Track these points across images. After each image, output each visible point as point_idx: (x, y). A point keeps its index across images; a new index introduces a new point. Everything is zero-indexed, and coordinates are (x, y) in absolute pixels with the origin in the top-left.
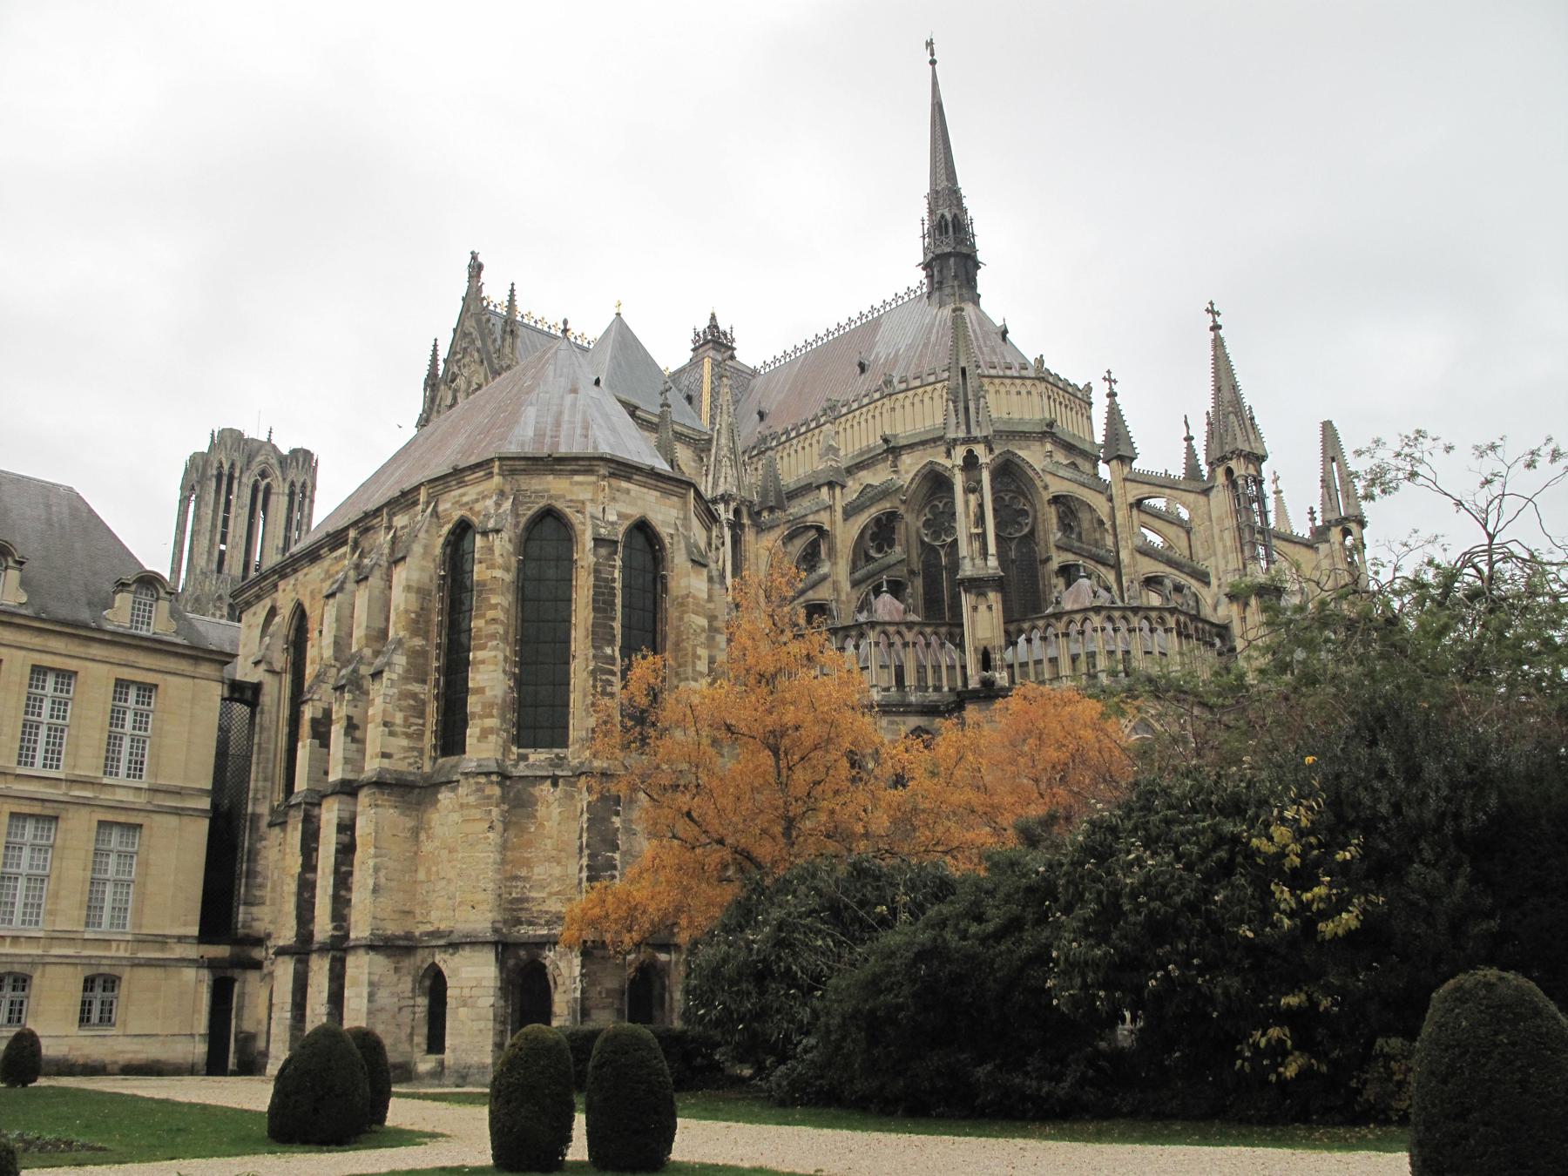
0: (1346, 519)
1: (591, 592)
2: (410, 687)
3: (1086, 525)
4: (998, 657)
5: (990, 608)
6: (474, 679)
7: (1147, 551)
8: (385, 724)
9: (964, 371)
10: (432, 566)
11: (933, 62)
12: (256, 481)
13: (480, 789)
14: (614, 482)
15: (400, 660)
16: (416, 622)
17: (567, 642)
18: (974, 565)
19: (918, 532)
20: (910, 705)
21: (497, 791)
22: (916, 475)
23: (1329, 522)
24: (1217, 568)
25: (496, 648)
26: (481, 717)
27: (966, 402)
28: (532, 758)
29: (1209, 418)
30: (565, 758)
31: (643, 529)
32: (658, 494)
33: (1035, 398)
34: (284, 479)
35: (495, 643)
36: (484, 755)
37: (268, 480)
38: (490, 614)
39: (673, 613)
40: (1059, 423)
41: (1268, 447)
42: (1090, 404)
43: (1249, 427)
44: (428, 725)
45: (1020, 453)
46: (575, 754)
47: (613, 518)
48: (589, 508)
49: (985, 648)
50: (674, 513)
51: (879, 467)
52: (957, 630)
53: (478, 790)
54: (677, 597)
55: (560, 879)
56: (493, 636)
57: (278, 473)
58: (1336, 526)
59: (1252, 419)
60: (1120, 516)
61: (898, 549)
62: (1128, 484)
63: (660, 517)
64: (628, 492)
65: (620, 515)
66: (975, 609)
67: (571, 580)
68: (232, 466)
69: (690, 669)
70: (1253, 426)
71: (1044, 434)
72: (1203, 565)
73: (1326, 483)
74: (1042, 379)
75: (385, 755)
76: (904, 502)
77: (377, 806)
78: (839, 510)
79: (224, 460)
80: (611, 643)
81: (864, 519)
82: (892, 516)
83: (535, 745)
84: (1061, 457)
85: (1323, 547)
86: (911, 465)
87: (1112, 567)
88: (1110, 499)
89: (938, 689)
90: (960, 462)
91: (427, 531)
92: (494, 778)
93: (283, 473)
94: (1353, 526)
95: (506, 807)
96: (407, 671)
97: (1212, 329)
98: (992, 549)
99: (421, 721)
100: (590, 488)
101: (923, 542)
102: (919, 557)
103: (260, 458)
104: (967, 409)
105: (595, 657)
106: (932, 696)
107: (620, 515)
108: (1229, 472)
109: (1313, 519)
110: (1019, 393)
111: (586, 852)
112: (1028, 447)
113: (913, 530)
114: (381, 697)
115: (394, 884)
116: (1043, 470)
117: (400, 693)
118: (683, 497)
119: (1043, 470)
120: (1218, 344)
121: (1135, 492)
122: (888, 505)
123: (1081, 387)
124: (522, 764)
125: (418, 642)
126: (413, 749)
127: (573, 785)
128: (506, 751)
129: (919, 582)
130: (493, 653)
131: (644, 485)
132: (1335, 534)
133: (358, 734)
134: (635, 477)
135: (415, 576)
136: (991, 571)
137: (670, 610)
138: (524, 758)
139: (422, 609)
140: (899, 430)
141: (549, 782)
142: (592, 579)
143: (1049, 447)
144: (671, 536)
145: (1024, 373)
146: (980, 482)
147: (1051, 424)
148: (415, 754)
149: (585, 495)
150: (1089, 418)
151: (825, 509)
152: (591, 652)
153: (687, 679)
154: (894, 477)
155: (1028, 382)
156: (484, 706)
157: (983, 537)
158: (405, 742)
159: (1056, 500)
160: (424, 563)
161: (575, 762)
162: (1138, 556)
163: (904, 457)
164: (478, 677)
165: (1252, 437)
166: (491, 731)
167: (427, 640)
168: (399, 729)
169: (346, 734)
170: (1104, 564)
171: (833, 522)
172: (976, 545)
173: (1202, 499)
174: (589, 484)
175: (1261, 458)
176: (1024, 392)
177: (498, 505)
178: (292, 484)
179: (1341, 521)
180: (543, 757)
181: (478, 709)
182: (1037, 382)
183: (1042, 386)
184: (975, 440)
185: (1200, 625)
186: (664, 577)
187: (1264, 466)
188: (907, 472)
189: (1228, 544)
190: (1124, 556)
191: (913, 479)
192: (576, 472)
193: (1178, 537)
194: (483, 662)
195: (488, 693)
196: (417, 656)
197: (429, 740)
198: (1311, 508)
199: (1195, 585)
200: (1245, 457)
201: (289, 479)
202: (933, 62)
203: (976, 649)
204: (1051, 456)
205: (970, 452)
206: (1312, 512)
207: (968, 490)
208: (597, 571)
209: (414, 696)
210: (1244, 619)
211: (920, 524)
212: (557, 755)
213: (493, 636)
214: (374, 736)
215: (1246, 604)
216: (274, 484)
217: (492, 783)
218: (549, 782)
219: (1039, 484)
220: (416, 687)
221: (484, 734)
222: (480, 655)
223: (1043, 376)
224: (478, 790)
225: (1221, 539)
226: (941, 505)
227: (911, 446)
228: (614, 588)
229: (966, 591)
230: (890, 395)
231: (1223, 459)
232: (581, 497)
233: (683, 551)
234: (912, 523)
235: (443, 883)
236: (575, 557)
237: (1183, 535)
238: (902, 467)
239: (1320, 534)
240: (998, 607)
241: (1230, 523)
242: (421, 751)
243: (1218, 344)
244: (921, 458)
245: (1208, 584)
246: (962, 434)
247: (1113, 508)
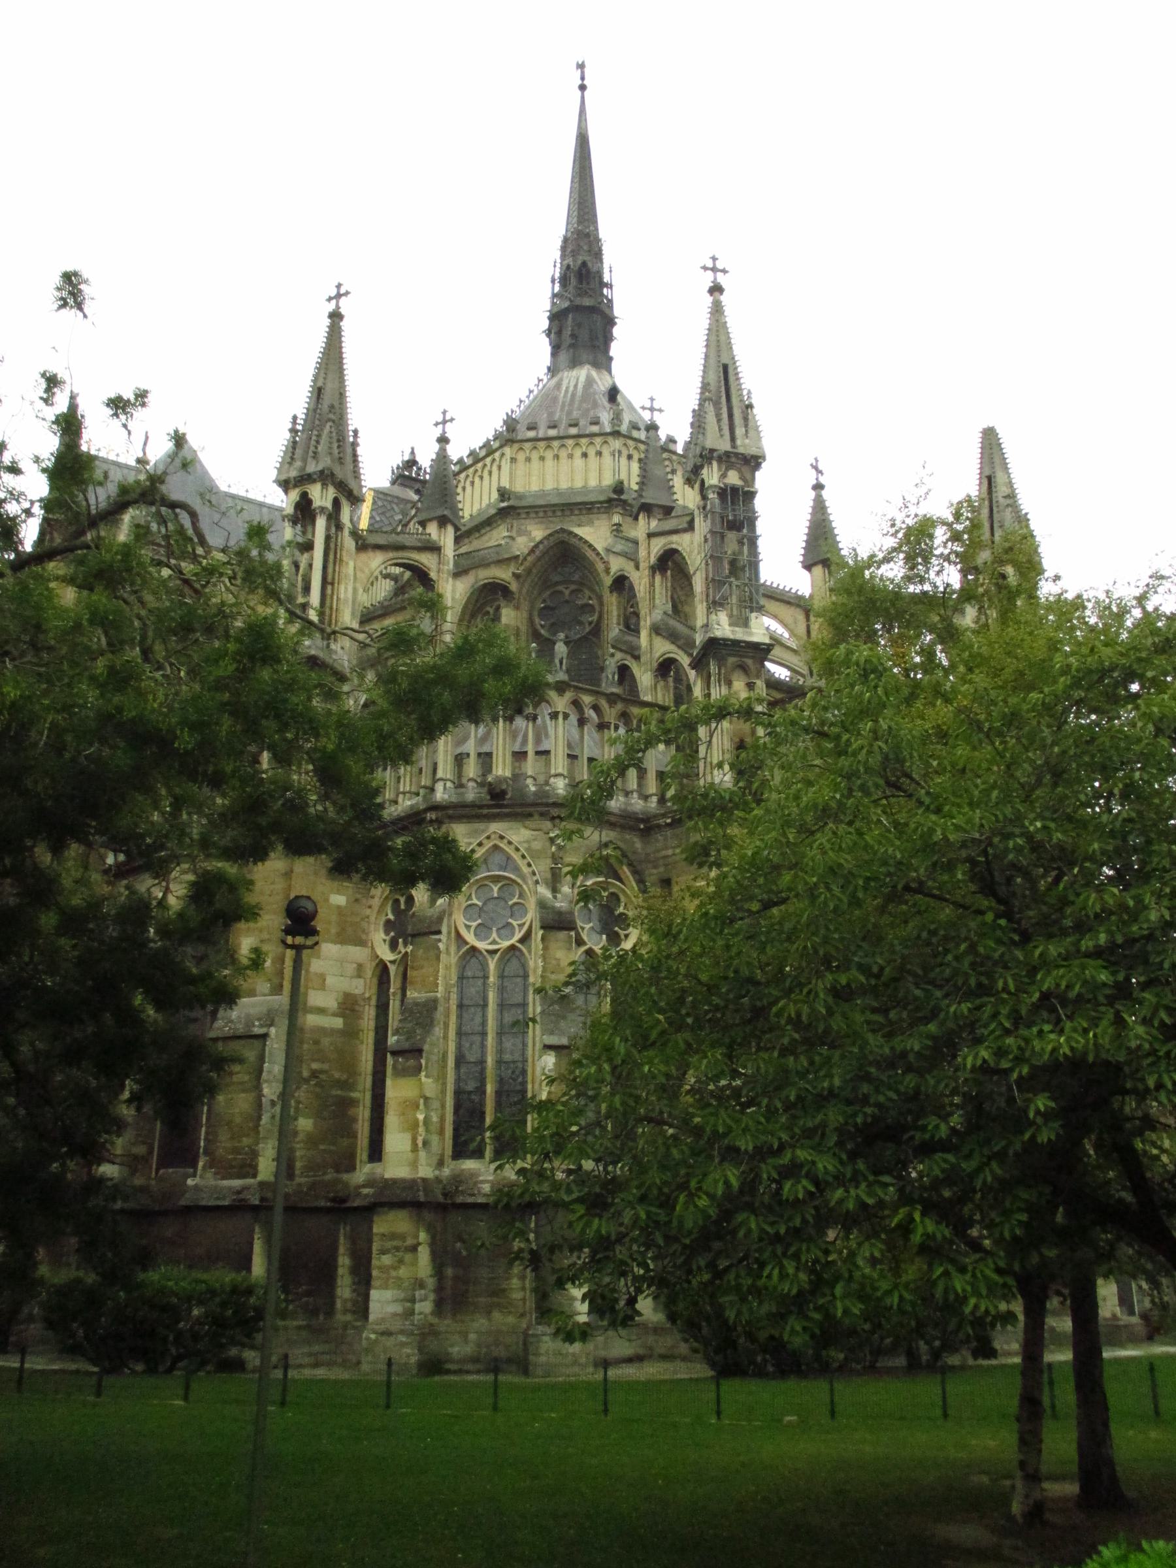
11: (583, 88)
33: (607, 459)
40: (626, 483)
45: (579, 531)
59: (750, 406)
71: (610, 501)
110: (585, 455)
112: (590, 523)
116: (608, 550)
143: (616, 519)
176: (592, 452)
182: (610, 439)
183: (616, 444)
200: (720, 460)
202: (583, 88)
219: (600, 567)
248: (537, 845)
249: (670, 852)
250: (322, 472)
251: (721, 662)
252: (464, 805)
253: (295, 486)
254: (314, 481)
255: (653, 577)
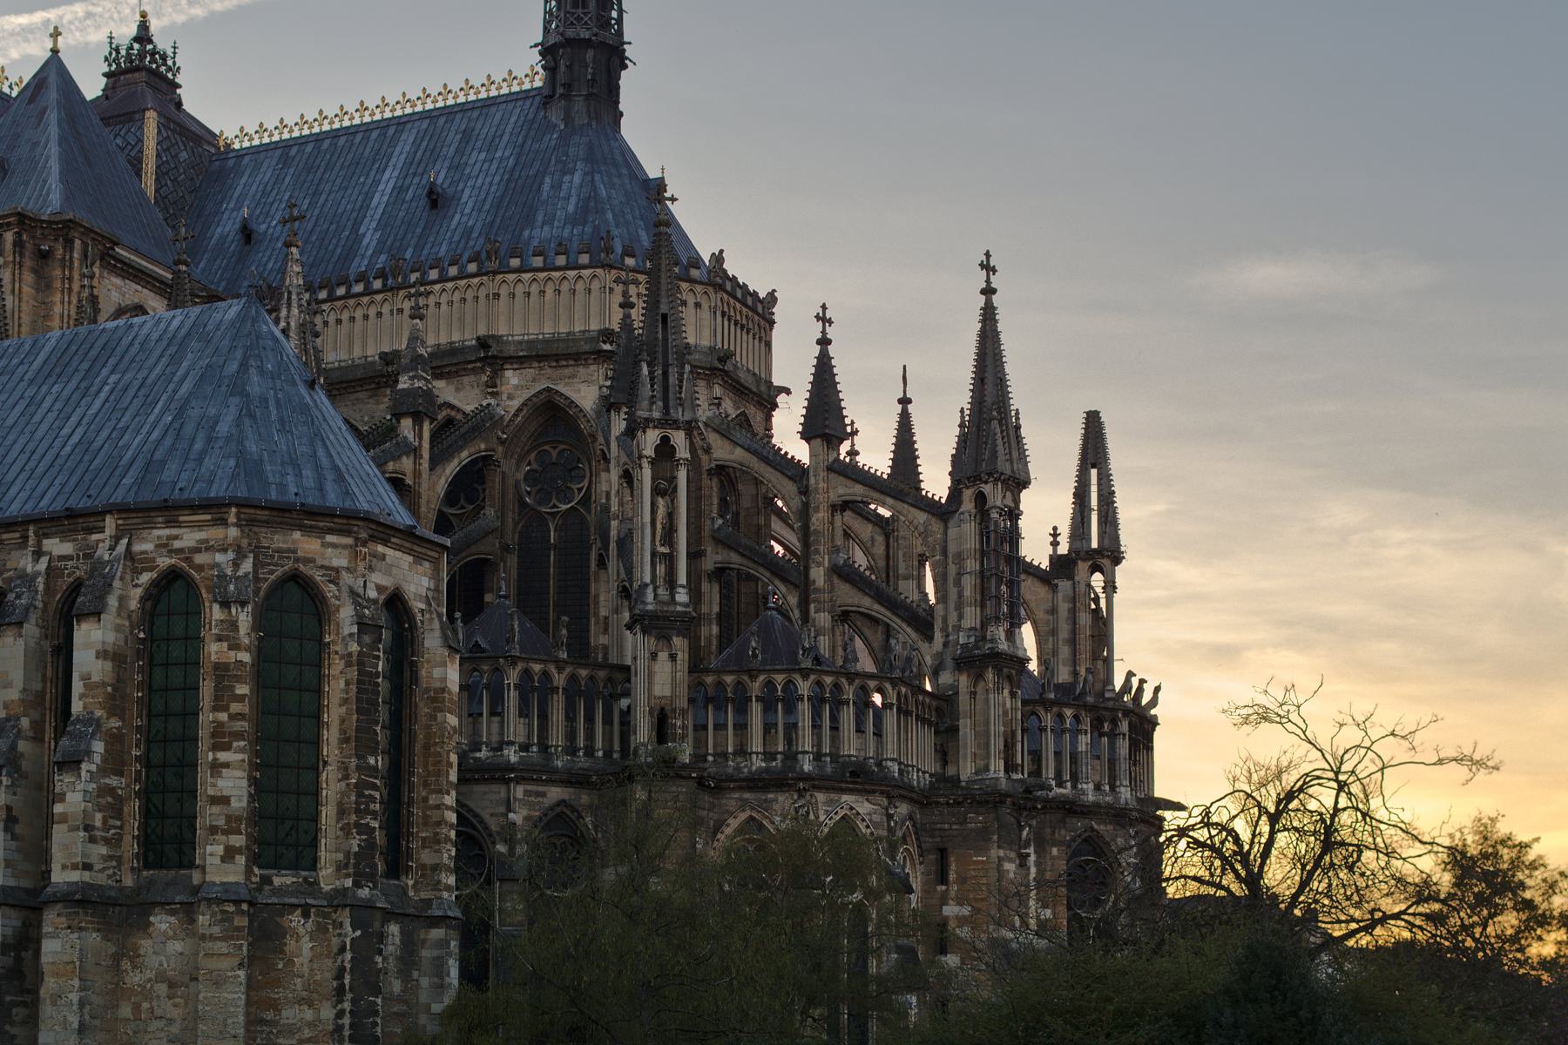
0: (1098, 552)
1: (354, 688)
2: (107, 781)
3: (746, 502)
4: (679, 723)
5: (673, 657)
6: (214, 785)
7: (845, 573)
8: (87, 828)
9: (665, 317)
10: (127, 623)
13: (226, 918)
14: (371, 545)
15: (98, 747)
16: (111, 697)
17: (317, 743)
18: (656, 596)
19: (517, 486)
20: (555, 771)
21: (245, 922)
22: (524, 404)
23: (1078, 553)
24: (945, 620)
25: (241, 750)
26: (226, 832)
27: (666, 367)
28: (277, 881)
29: (962, 417)
30: (316, 883)
31: (395, 602)
32: (410, 559)
33: (705, 314)
35: (242, 743)
36: (232, 879)
38: (235, 707)
39: (424, 710)
41: (1034, 469)
42: (772, 323)
43: (1012, 433)
44: (127, 828)
46: (328, 877)
47: (372, 594)
48: (346, 578)
49: (662, 709)
50: (425, 582)
51: (466, 380)
52: (619, 676)
53: (222, 920)
54: (428, 690)
55: (311, 1025)
56: (239, 735)
58: (1084, 560)
59: (1018, 427)
60: (819, 518)
61: (490, 512)
62: (832, 476)
63: (412, 588)
64: (383, 557)
65: (380, 588)
66: (654, 656)
67: (319, 666)
69: (443, 780)
70: (1019, 438)
72: (907, 590)
73: (1081, 496)
74: (721, 288)
75: (87, 867)
76: (502, 442)
77: (81, 929)
78: (426, 455)
80: (374, 753)
81: (451, 468)
82: (486, 461)
83: (276, 864)
84: (729, 408)
85: (1064, 585)
86: (517, 387)
87: (796, 586)
88: (805, 491)
89: (590, 751)
90: (649, 451)
91: (122, 579)
92: (245, 907)
94: (1106, 562)
95: (250, 939)
96: (104, 760)
97: (983, 292)
98: (682, 578)
99: (119, 823)
100: (346, 552)
101: (522, 504)
102: (516, 525)
104: (665, 374)
105: (358, 768)
106: (582, 761)
107: (380, 588)
108: (981, 498)
109: (1055, 544)
111: (349, 996)
113: (511, 482)
114: (74, 796)
115: (97, 1022)
116: (706, 424)
117: (99, 788)
118: (435, 563)
119: (706, 424)
120: (989, 315)
121: (841, 491)
122: (483, 446)
123: (762, 295)
124: (267, 888)
125: (115, 723)
126: (111, 858)
127: (326, 916)
128: (248, 872)
129: (513, 561)
130: (240, 756)
131: (398, 548)
132: (1082, 567)
133: (18, 829)
134: (393, 540)
135: (111, 637)
136: (679, 608)
137: (421, 705)
138: (266, 880)
139: (118, 681)
140: (503, 331)
141: (299, 911)
142: (354, 673)
143: (718, 391)
144: (422, 611)
145: (694, 273)
146: (673, 480)
147: (726, 357)
148: (114, 863)
149: (340, 561)
150: (768, 345)
151: (407, 454)
152: (354, 762)
153: (439, 791)
154: (493, 401)
155: (699, 288)
156: (229, 818)
157: (670, 560)
158: (103, 850)
159: (721, 470)
160: (118, 621)
161: (326, 888)
162: (836, 580)
163: (509, 373)
164: (221, 783)
165: (1015, 454)
166: (239, 851)
167: (123, 721)
168: (98, 833)
169: (6, 830)
170: (784, 580)
171: (417, 474)
172: (661, 569)
173: (936, 526)
174: (345, 547)
175: (1024, 483)
177: (236, 565)
179: (1091, 554)
180: (289, 880)
181: (221, 822)
182: (711, 290)
184: (676, 425)
185: (921, 698)
186: (413, 664)
187: (1025, 496)
188: (510, 397)
189: (967, 593)
190: (818, 575)
191: (519, 410)
192: (331, 531)
193: (873, 539)
194: (227, 765)
195: (235, 804)
196: (115, 740)
197: (130, 847)
198: (1055, 529)
199: (906, 634)
203: (651, 713)
204: (719, 405)
205: (665, 440)
206: (1055, 535)
207: (657, 491)
208: (360, 663)
209: (111, 791)
210: (973, 694)
211: (521, 476)
212: (305, 879)
213: (239, 735)
214: (65, 844)
215: (979, 677)
217: (243, 912)
218: (299, 911)
220: (113, 781)
221: (229, 855)
222: (223, 756)
223: (718, 279)
224: (222, 920)
225: (958, 583)
226: (554, 453)
227: (520, 361)
228: (377, 684)
229: (644, 632)
230: (495, 273)
231: (976, 479)
232: (336, 563)
233: (437, 633)
234: (512, 472)
235: (155, 1025)
236: (327, 639)
237: (880, 539)
238: (505, 389)
239: (1061, 565)
240: (683, 657)
241: (972, 565)
242: (119, 860)
243: (989, 315)
244: (534, 380)
245: (929, 638)
246: (656, 415)
247: (806, 505)
248: (876, 818)
249: (946, 826)
250: (689, 422)
251: (998, 671)
252: (823, 778)
253: (655, 427)
254: (678, 428)
255: (833, 516)
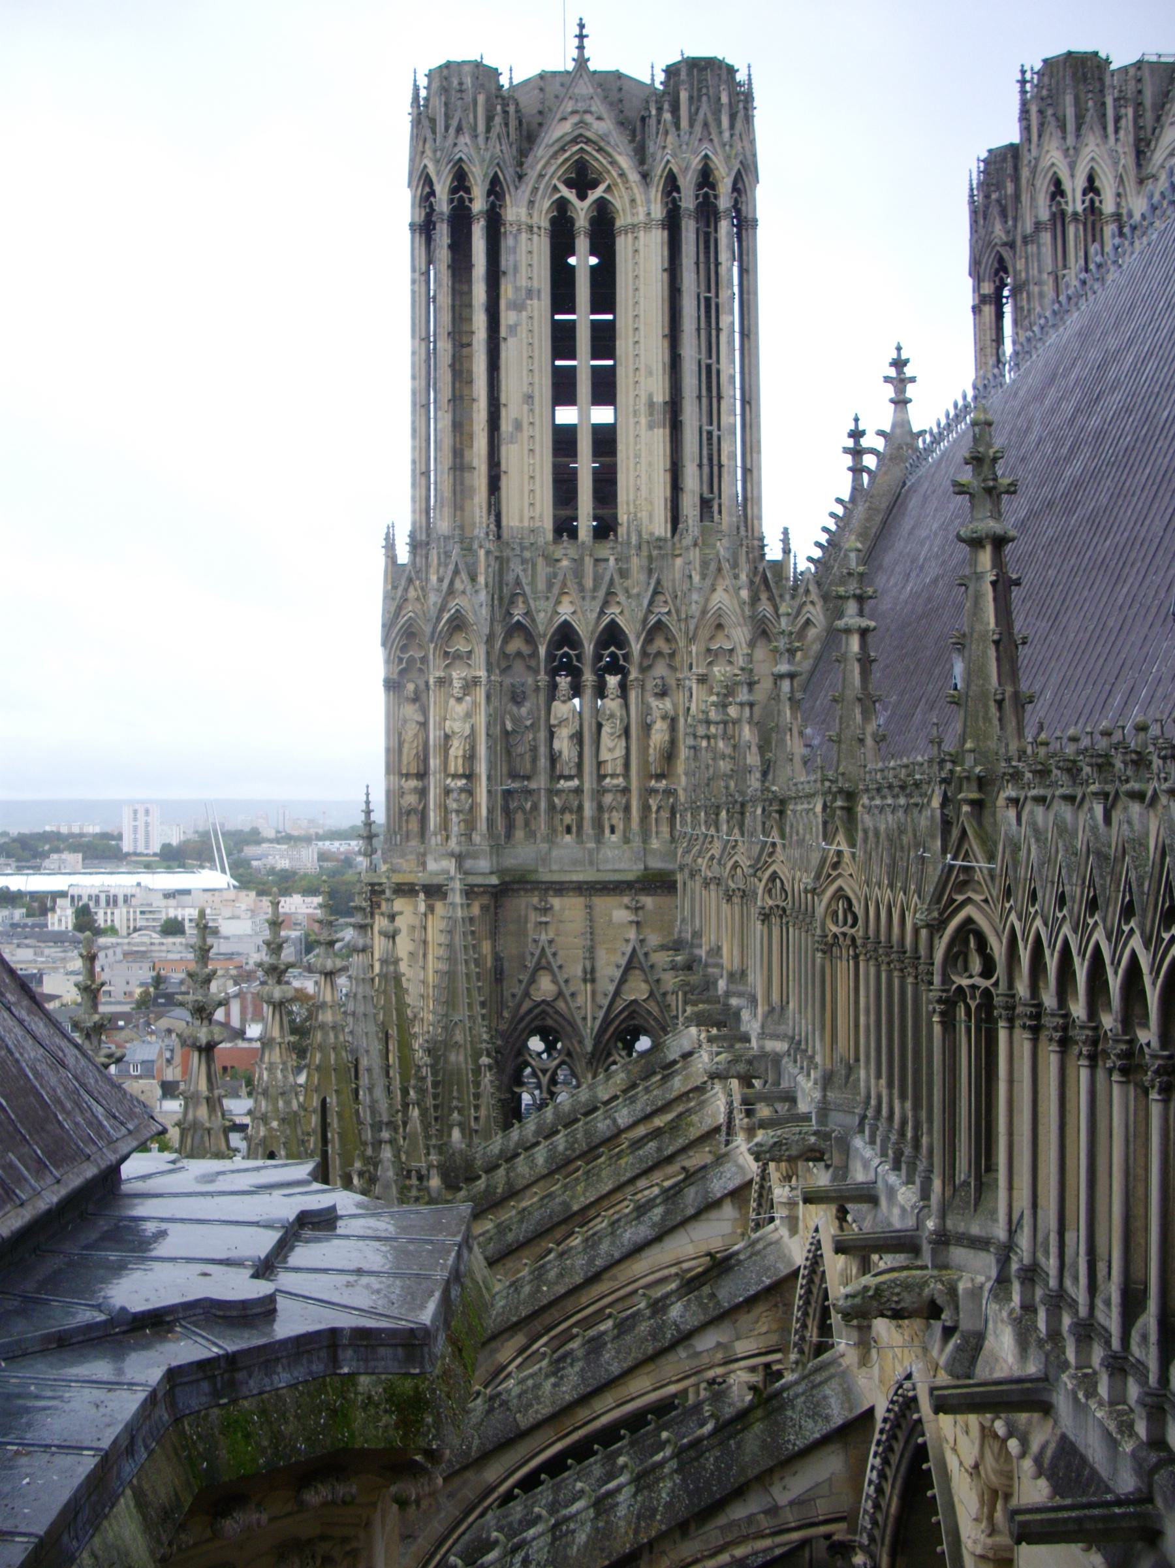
12: (562, 205)
34: (645, 176)
37: (598, 192)
57: (625, 162)
68: (460, 182)
79: (431, 170)
93: (641, 155)
103: (560, 130)
178: (672, 184)
201: (658, 171)
216: (619, 201)
